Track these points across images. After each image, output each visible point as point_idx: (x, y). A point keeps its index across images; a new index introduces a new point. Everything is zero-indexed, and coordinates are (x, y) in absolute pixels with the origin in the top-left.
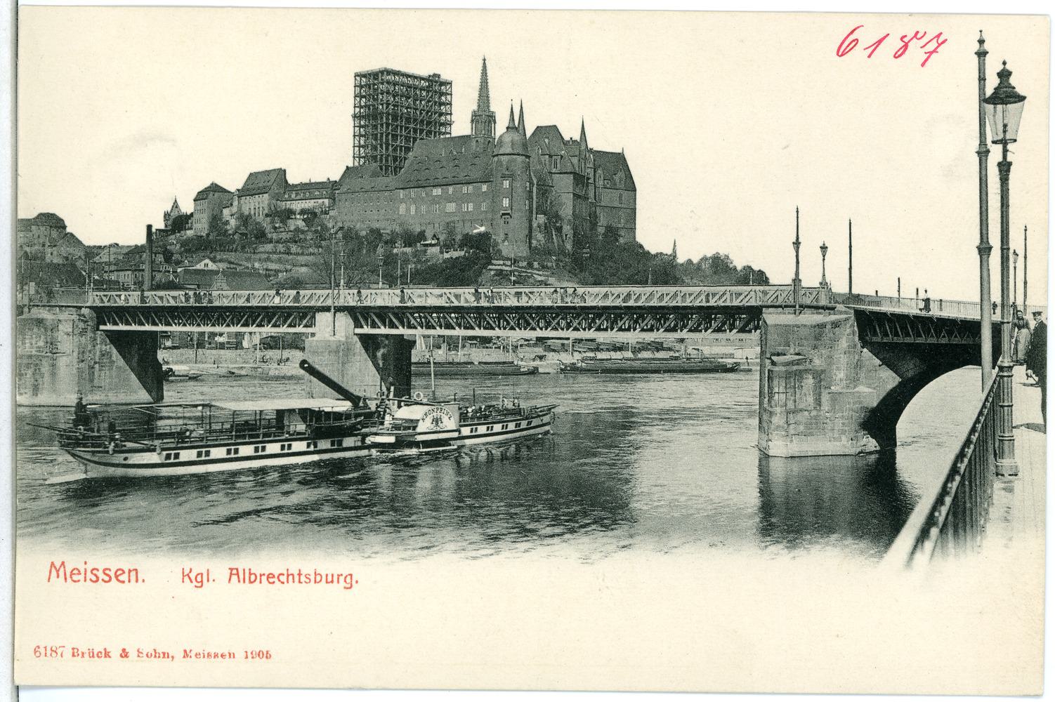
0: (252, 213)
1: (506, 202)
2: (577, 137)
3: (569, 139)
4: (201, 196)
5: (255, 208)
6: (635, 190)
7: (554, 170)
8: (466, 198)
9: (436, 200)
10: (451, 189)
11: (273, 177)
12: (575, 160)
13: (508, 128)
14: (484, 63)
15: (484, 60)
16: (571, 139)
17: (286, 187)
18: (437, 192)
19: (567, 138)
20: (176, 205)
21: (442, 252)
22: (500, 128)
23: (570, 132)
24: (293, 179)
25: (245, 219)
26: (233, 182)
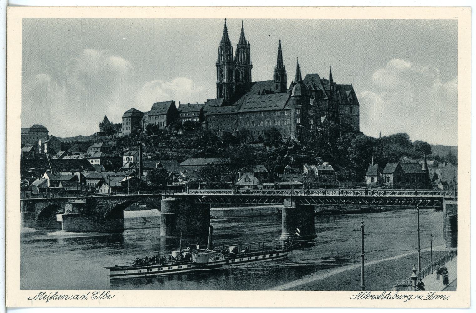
0: (157, 123)
1: (299, 121)
2: (327, 78)
3: (322, 79)
5: (159, 123)
6: (359, 105)
11: (168, 106)
15: (280, 41)
16: (323, 78)
19: (322, 78)
20: (106, 119)
21: (265, 146)
22: (291, 78)
24: (177, 106)
25: (153, 128)
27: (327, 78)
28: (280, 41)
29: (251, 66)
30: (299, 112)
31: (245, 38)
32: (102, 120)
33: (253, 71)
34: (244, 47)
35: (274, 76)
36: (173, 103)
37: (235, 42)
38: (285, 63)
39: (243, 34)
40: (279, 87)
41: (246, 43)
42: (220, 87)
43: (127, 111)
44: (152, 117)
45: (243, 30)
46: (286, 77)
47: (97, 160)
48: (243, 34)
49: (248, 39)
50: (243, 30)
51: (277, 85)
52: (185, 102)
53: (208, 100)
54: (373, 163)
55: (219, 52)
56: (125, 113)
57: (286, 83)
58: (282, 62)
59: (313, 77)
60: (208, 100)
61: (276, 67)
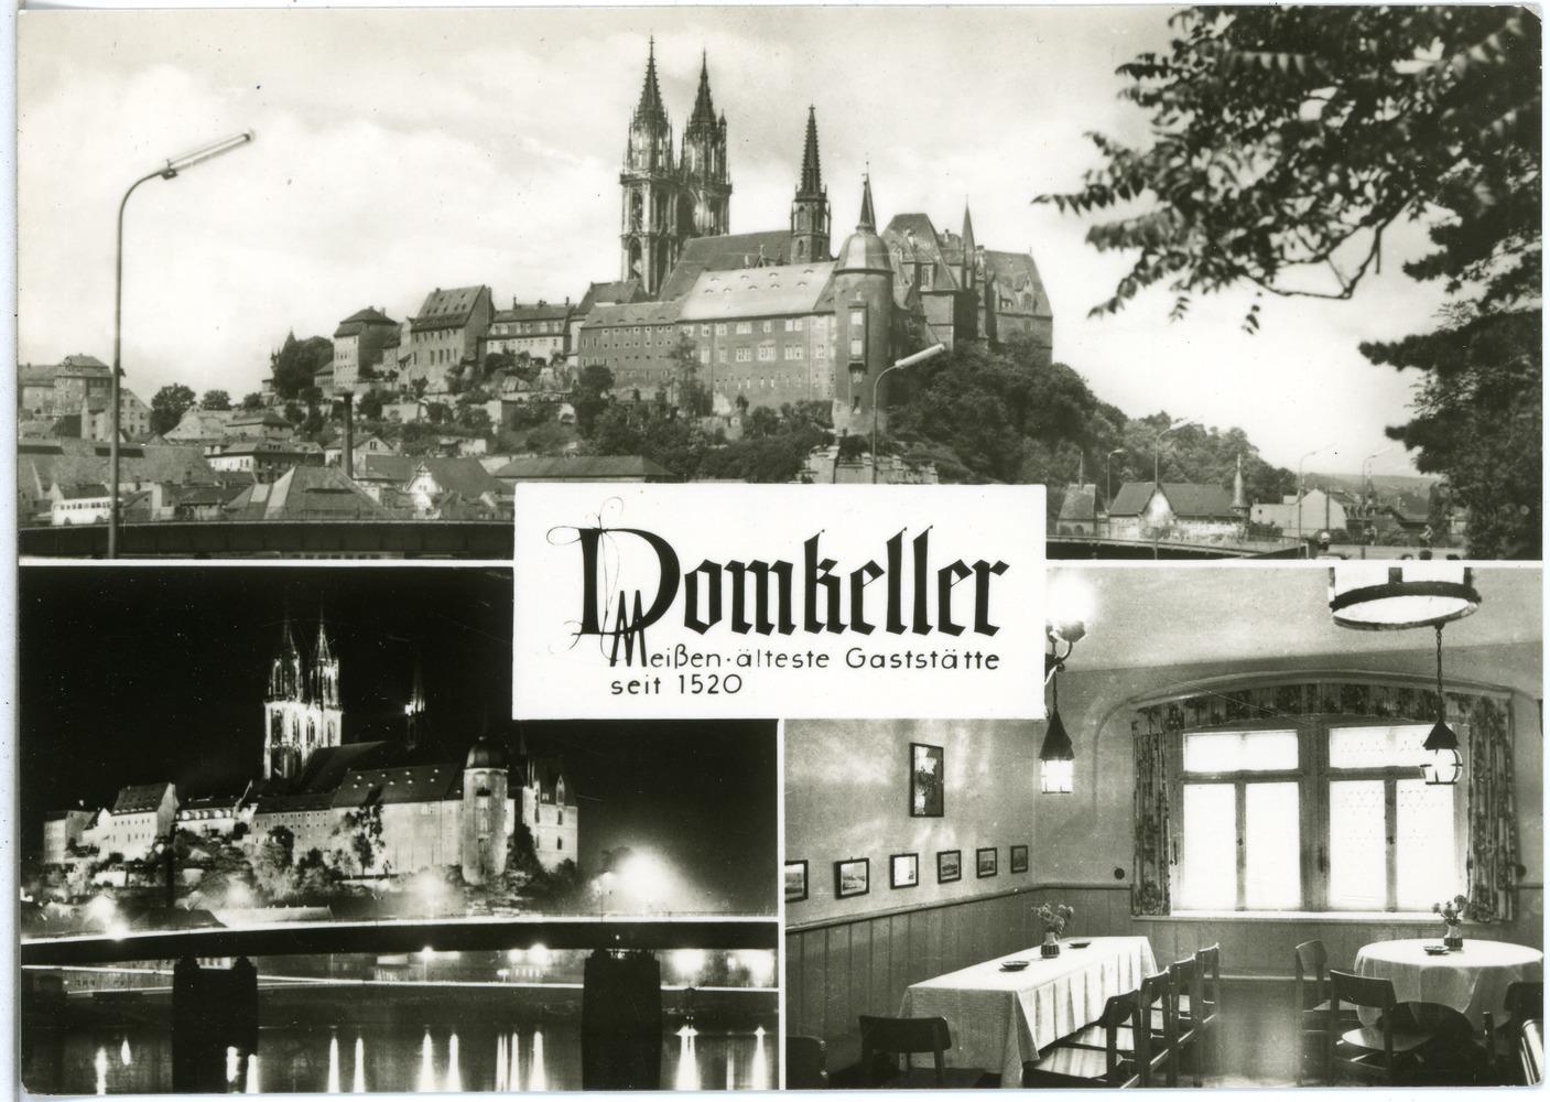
1: (857, 348)
2: (958, 230)
3: (943, 232)
4: (347, 329)
7: (923, 288)
8: (797, 339)
9: (745, 343)
10: (768, 326)
11: (468, 300)
12: (957, 272)
13: (858, 228)
14: (812, 112)
15: (812, 109)
16: (947, 231)
17: (492, 317)
18: (744, 329)
19: (940, 230)
22: (843, 223)
23: (946, 220)
24: (502, 302)
26: (402, 304)
27: (958, 230)
28: (812, 109)
29: (728, 190)
30: (857, 318)
31: (710, 104)
32: (279, 345)
33: (735, 201)
34: (708, 126)
35: (793, 214)
37: (679, 115)
38: (830, 181)
40: (807, 247)
41: (712, 116)
42: (633, 247)
43: (352, 317)
44: (421, 335)
46: (830, 218)
47: (245, 458)
49: (718, 108)
51: (801, 242)
52: (529, 298)
53: (593, 286)
54: (1080, 481)
56: (342, 323)
57: (828, 238)
58: (818, 175)
59: (913, 222)
60: (593, 286)
61: (800, 187)
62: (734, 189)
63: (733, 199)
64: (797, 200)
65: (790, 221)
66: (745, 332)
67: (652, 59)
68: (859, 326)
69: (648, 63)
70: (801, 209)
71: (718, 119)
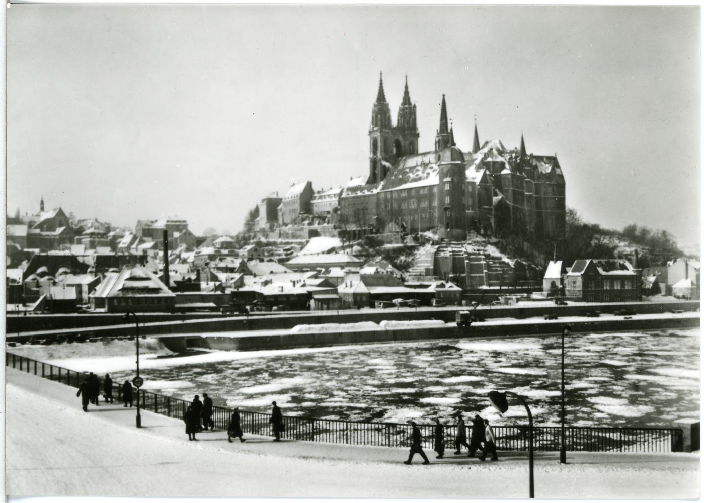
1: (447, 200)
15: (444, 95)
28: (444, 95)
29: (418, 136)
31: (409, 99)
34: (409, 111)
35: (436, 143)
36: (309, 185)
39: (406, 93)
41: (410, 104)
45: (406, 87)
48: (406, 93)
49: (412, 101)
50: (406, 87)
55: (373, 117)
61: (439, 131)
62: (420, 135)
63: (420, 140)
64: (437, 137)
65: (434, 146)
66: (404, 195)
67: (381, 81)
68: (447, 190)
69: (379, 82)
70: (439, 140)
71: (413, 104)
